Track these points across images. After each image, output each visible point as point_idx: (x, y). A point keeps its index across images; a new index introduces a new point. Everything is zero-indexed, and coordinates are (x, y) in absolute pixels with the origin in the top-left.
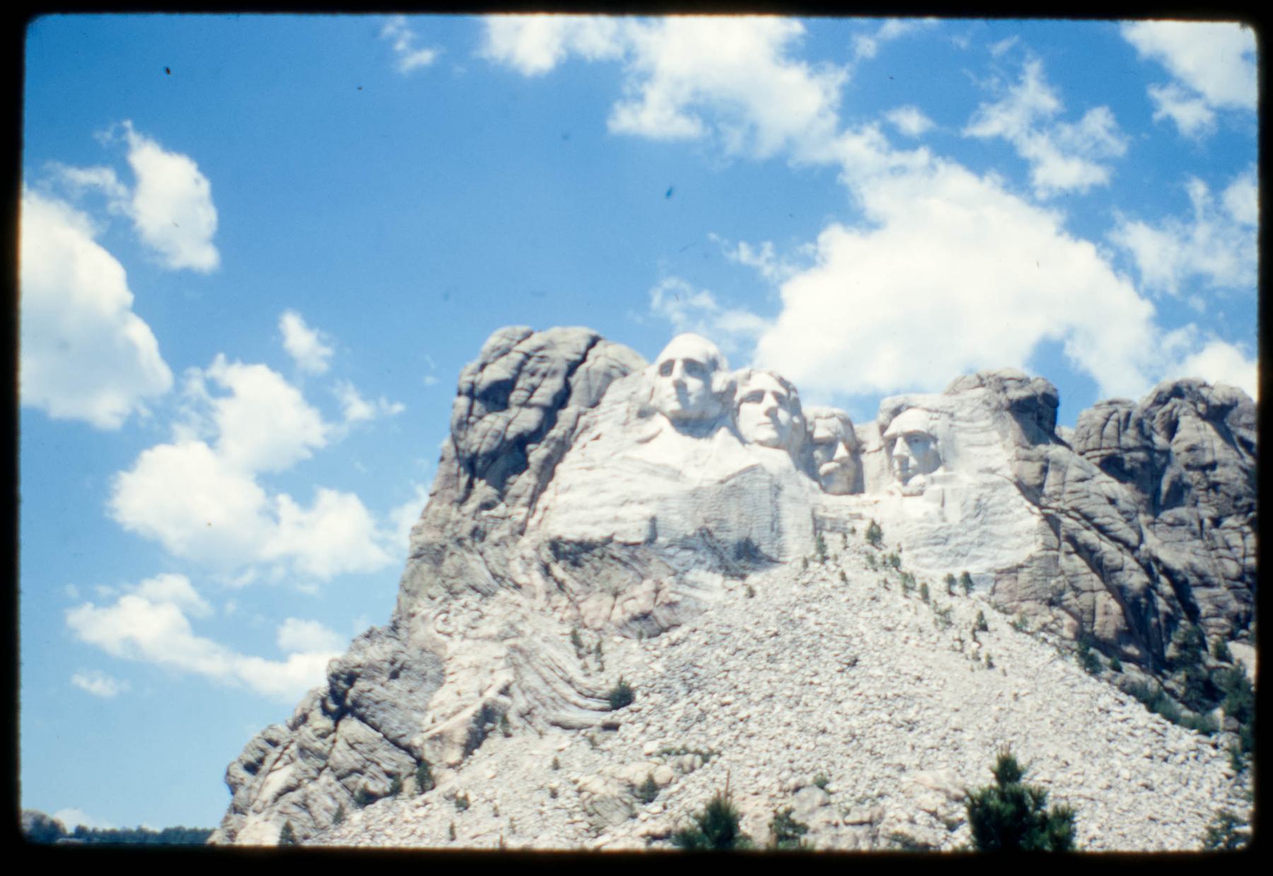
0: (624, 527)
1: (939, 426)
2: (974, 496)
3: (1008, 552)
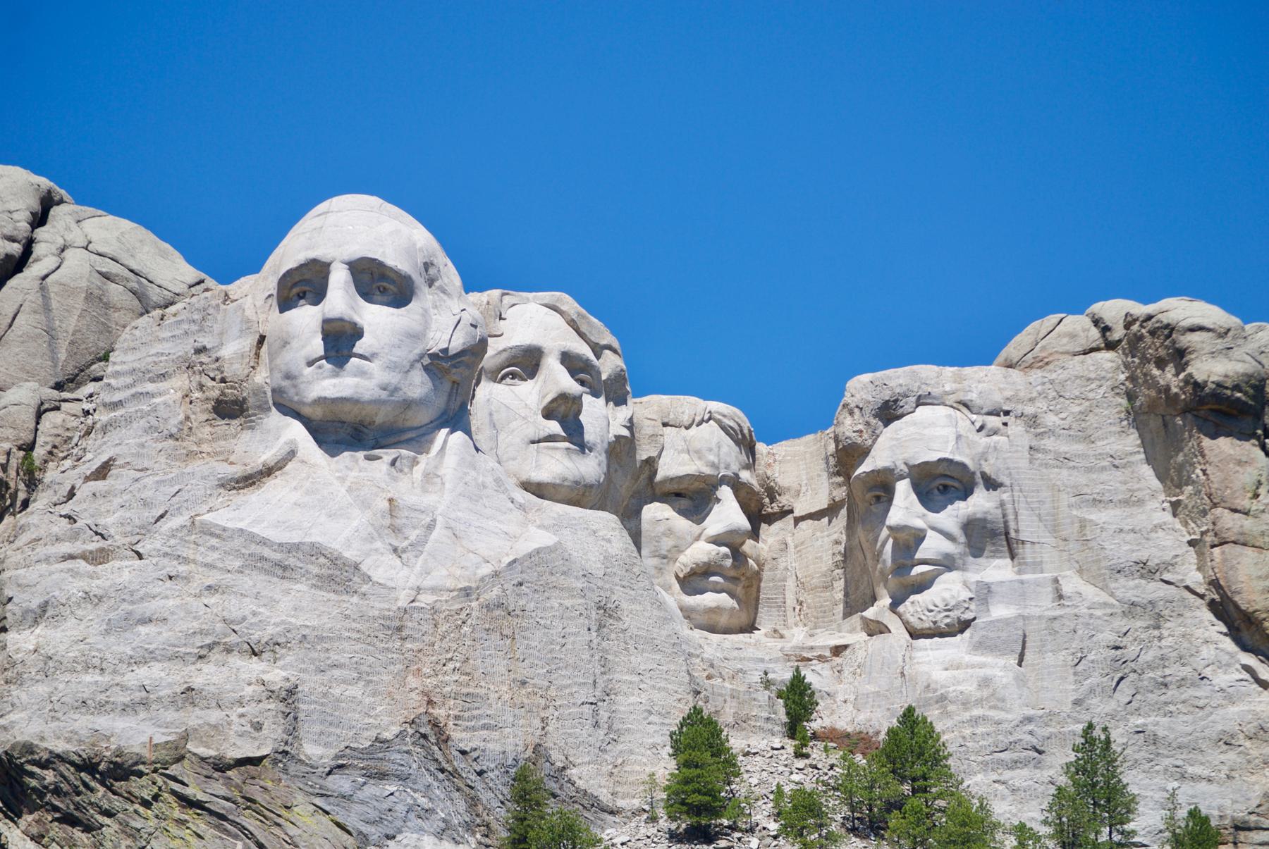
0: (215, 716)
1: (1004, 451)
2: (1109, 637)
3: (1203, 786)
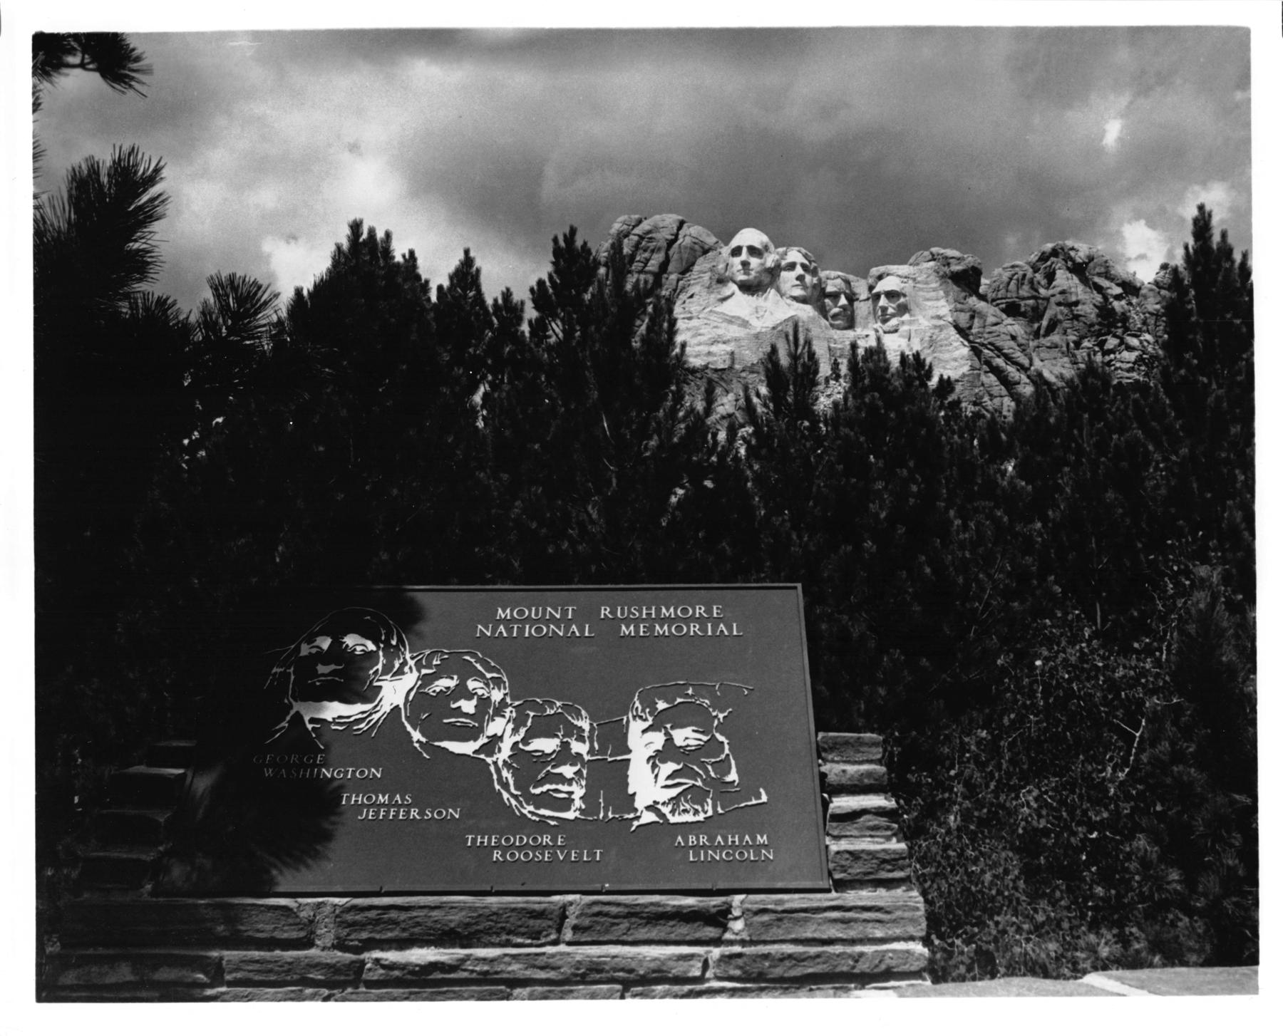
1: (908, 287)
